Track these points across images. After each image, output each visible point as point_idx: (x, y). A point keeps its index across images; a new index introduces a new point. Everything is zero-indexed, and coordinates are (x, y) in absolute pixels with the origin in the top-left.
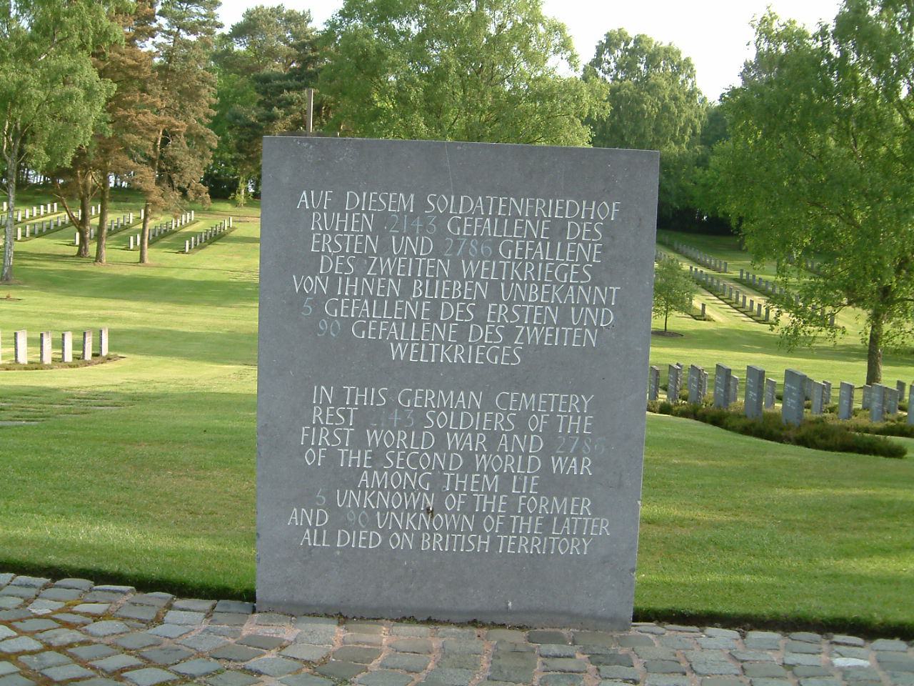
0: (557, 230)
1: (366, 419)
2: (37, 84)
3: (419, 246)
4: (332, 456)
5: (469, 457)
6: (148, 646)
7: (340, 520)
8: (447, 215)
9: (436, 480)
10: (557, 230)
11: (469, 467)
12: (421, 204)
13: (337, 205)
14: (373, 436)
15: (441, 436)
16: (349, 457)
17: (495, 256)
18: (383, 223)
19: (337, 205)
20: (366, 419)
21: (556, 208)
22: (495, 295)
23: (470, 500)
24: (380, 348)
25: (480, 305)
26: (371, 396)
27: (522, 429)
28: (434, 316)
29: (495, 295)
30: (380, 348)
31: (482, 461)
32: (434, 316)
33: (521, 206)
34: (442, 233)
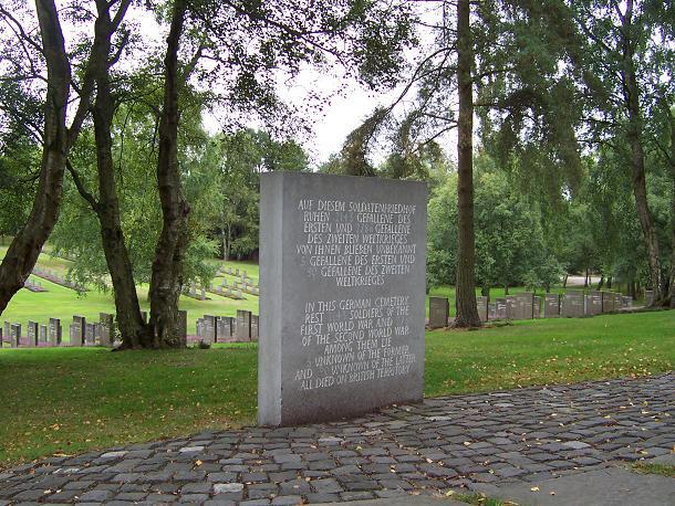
0: (395, 219)
1: (327, 318)
2: (419, 28)
3: (346, 228)
4: (314, 338)
5: (366, 330)
6: (617, 312)
7: (319, 374)
8: (357, 213)
9: (354, 346)
10: (395, 219)
11: (366, 338)
12: (347, 208)
13: (315, 208)
14: (330, 327)
15: (356, 321)
16: (323, 339)
17: (374, 232)
18: (333, 215)
19: (315, 208)
20: (327, 318)
21: (396, 208)
22: (374, 252)
23: (367, 353)
24: (332, 280)
25: (369, 258)
26: (326, 306)
27: (385, 316)
28: (353, 262)
29: (374, 252)
30: (332, 280)
31: (372, 333)
32: (353, 262)
33: (383, 207)
34: (355, 220)
